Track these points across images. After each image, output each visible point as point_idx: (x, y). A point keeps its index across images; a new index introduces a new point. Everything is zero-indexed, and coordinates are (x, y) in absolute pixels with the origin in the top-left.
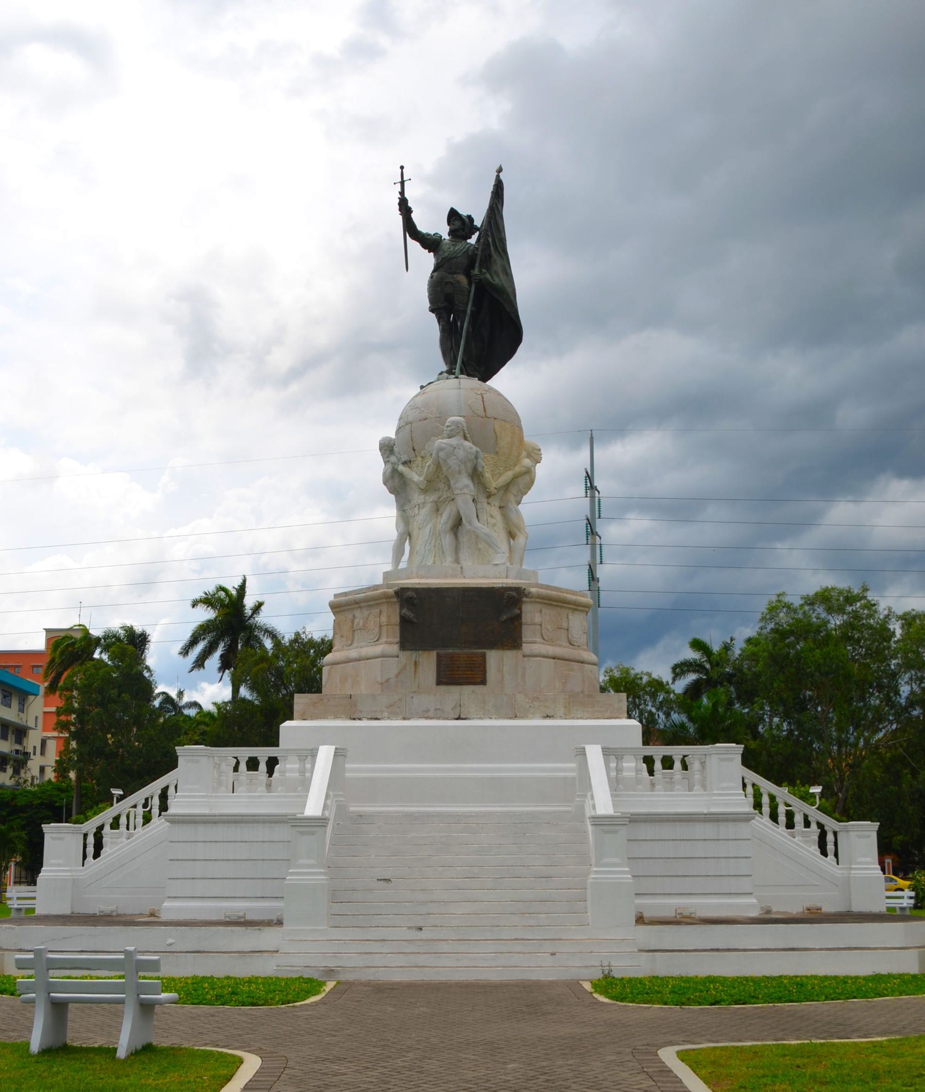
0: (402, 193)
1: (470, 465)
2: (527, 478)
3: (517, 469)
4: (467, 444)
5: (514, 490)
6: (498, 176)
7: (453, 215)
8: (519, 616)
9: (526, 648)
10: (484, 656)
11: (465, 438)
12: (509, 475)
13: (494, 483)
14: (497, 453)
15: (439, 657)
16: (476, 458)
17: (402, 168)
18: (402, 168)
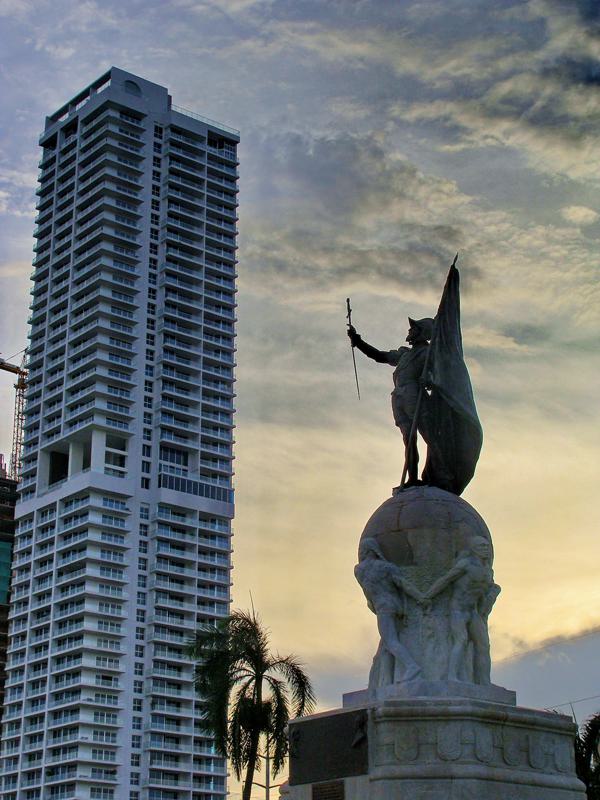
0: (349, 325)
1: (384, 582)
2: (466, 579)
3: (450, 573)
4: (377, 562)
5: (457, 594)
6: (453, 267)
7: (412, 322)
8: (364, 739)
9: (376, 772)
10: (342, 784)
11: (377, 557)
12: (440, 582)
13: (422, 596)
14: (416, 564)
15: (314, 789)
16: (388, 574)
17: (348, 300)
18: (348, 300)
